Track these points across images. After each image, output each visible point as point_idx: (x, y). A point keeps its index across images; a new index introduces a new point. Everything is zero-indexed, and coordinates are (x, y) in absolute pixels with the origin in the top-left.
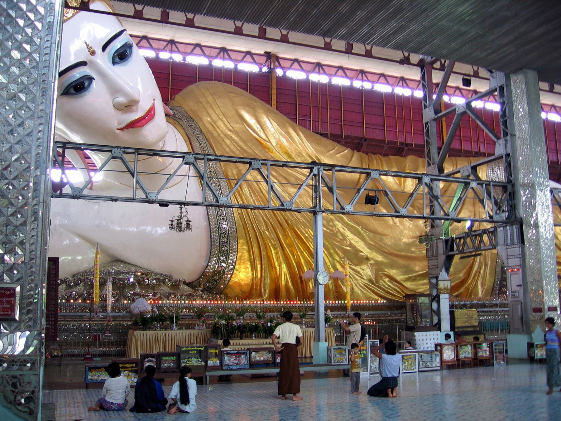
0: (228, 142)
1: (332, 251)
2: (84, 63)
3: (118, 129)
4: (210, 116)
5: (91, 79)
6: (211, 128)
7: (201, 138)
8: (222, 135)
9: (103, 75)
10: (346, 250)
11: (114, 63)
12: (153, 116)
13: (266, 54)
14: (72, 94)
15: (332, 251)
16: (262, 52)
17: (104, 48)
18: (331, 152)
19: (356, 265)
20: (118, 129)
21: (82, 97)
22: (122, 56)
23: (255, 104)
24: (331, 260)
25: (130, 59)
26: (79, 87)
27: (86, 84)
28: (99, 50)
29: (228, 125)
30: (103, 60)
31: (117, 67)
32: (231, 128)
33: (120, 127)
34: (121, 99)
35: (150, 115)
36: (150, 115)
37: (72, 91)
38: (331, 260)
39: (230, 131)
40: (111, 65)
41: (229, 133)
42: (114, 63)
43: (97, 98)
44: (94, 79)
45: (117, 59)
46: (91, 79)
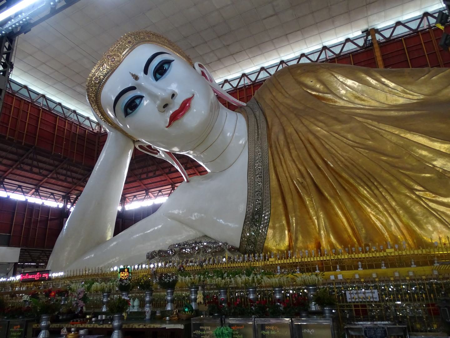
2: (133, 88)
3: (167, 127)
4: (271, 93)
5: (141, 97)
7: (258, 113)
11: (157, 79)
14: (131, 113)
15: (395, 184)
16: (359, 33)
17: (146, 72)
18: (423, 78)
20: (167, 127)
22: (161, 71)
26: (132, 106)
27: (137, 101)
28: (141, 74)
30: (147, 82)
31: (159, 82)
33: (167, 124)
35: (185, 106)
36: (185, 106)
37: (129, 111)
40: (154, 82)
42: (157, 79)
45: (158, 76)
46: (141, 97)
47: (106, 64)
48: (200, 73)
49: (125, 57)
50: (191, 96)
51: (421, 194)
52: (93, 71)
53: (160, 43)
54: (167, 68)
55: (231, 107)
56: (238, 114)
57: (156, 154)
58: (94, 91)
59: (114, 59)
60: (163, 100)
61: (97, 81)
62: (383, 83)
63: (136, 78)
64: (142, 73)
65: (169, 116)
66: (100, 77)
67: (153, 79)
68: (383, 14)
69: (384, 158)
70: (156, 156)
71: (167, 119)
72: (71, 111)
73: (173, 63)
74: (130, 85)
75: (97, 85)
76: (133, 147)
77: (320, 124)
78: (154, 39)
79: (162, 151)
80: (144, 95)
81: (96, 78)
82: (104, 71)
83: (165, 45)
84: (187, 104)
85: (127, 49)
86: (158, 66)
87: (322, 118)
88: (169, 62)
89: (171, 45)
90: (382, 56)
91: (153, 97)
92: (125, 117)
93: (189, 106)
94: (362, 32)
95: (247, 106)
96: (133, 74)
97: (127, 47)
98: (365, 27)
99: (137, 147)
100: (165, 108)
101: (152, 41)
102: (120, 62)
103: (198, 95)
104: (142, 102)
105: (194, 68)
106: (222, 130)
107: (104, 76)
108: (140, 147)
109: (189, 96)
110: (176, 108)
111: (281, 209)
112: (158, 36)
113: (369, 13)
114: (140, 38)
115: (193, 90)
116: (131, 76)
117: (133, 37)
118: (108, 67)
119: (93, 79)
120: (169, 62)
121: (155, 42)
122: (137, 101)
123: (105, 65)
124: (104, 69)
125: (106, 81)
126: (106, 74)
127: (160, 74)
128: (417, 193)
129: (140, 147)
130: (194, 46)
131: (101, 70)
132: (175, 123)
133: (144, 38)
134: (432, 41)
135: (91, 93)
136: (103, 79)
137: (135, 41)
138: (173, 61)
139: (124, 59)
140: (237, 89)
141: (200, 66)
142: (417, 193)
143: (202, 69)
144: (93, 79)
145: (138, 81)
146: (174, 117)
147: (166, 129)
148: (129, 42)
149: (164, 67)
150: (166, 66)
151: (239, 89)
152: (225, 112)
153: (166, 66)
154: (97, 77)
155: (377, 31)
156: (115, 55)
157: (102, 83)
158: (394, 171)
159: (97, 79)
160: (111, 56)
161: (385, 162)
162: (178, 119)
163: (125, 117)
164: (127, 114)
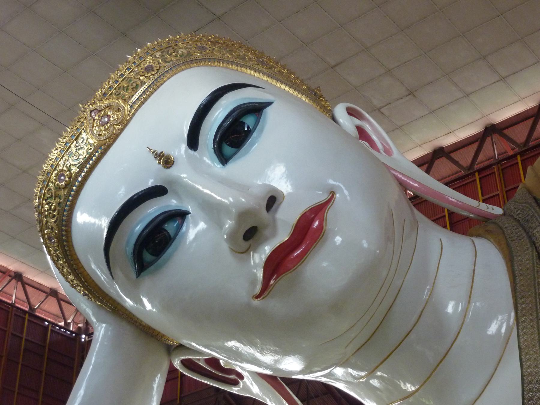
2: (157, 191)
5: (180, 215)
11: (224, 160)
17: (193, 141)
20: (257, 297)
21: (168, 259)
22: (234, 136)
27: (170, 227)
28: (180, 150)
31: (232, 166)
35: (308, 230)
36: (308, 230)
37: (147, 257)
40: (217, 166)
42: (224, 160)
44: (189, 213)
45: (227, 150)
46: (180, 215)
47: (87, 133)
48: (354, 132)
49: (136, 110)
52: (54, 154)
53: (232, 63)
54: (251, 128)
55: (457, 223)
57: (235, 383)
58: (54, 211)
59: (109, 117)
60: (243, 215)
61: (63, 180)
64: (184, 146)
65: (262, 264)
66: (69, 170)
67: (213, 162)
70: (235, 390)
71: (255, 275)
72: (10, 276)
73: (269, 112)
74: (150, 183)
75: (63, 193)
76: (165, 368)
78: (217, 54)
79: (251, 373)
80: (190, 209)
82: (80, 152)
83: (247, 67)
84: (312, 221)
85: (143, 89)
86: (226, 124)
88: (257, 109)
89: (263, 64)
91: (212, 210)
92: (139, 274)
93: (321, 227)
96: (159, 151)
97: (143, 83)
99: (177, 364)
100: (250, 242)
101: (209, 60)
102: (124, 124)
103: (346, 192)
104: (184, 229)
105: (334, 119)
107: (81, 167)
108: (187, 364)
109: (320, 197)
110: (283, 236)
112: (227, 46)
114: (176, 56)
115: (331, 182)
116: (152, 157)
117: (158, 54)
118: (91, 141)
119: (53, 178)
120: (257, 109)
121: (219, 61)
122: (170, 227)
123: (84, 135)
124: (81, 148)
125: (85, 179)
126: (86, 161)
127: (231, 145)
129: (187, 364)
130: (333, 63)
131: (74, 150)
133: (189, 54)
135: (46, 217)
136: (78, 174)
137: (163, 64)
138: (269, 104)
139: (134, 114)
140: (473, 174)
141: (351, 112)
143: (358, 122)
144: (53, 178)
145: (173, 171)
147: (256, 302)
148: (149, 69)
149: (244, 123)
150: (249, 121)
151: (480, 171)
153: (249, 121)
154: (62, 170)
156: (109, 107)
157: (74, 185)
159: (63, 175)
160: (100, 111)
162: (288, 270)
163: (139, 274)
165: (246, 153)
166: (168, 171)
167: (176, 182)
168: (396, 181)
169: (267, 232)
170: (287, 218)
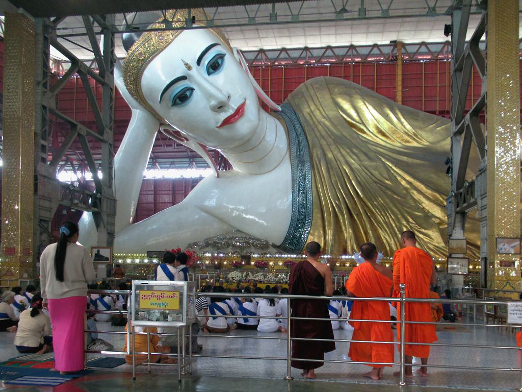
0: (320, 128)
1: (400, 216)
2: (183, 78)
3: (217, 127)
4: (309, 107)
5: (192, 90)
6: (308, 118)
8: (317, 123)
9: (199, 85)
10: (417, 215)
11: (209, 74)
12: (243, 111)
13: (392, 43)
15: (400, 216)
16: (388, 42)
18: (431, 126)
19: (425, 229)
20: (217, 127)
21: (186, 105)
22: (214, 67)
23: (353, 91)
24: (397, 224)
25: (221, 68)
26: (183, 98)
27: (188, 93)
29: (324, 113)
32: (325, 115)
34: (213, 103)
35: (240, 112)
36: (240, 112)
37: (178, 101)
38: (397, 224)
39: (324, 117)
40: (206, 75)
41: (323, 120)
42: (209, 74)
43: (198, 105)
45: (211, 70)
46: (192, 90)
50: (243, 101)
51: (413, 225)
56: (277, 121)
62: (402, 123)
63: (189, 68)
68: (413, 33)
69: (396, 197)
77: (355, 157)
81: (141, 54)
87: (355, 151)
90: (403, 75)
91: (209, 96)
92: (172, 106)
94: (391, 42)
95: (282, 112)
96: (186, 62)
98: (394, 37)
106: (264, 137)
111: (320, 222)
113: (402, 29)
116: (183, 64)
125: (151, 60)
128: (411, 224)
132: (226, 127)
134: (445, 100)
142: (411, 224)
146: (228, 122)
147: (217, 129)
152: (265, 115)
155: (404, 45)
158: (399, 206)
161: (396, 199)
163: (172, 106)
164: (175, 104)
165: (218, 74)
166: (189, 71)
167: (190, 76)
168: (253, 90)
169: (226, 108)
170: (234, 105)
